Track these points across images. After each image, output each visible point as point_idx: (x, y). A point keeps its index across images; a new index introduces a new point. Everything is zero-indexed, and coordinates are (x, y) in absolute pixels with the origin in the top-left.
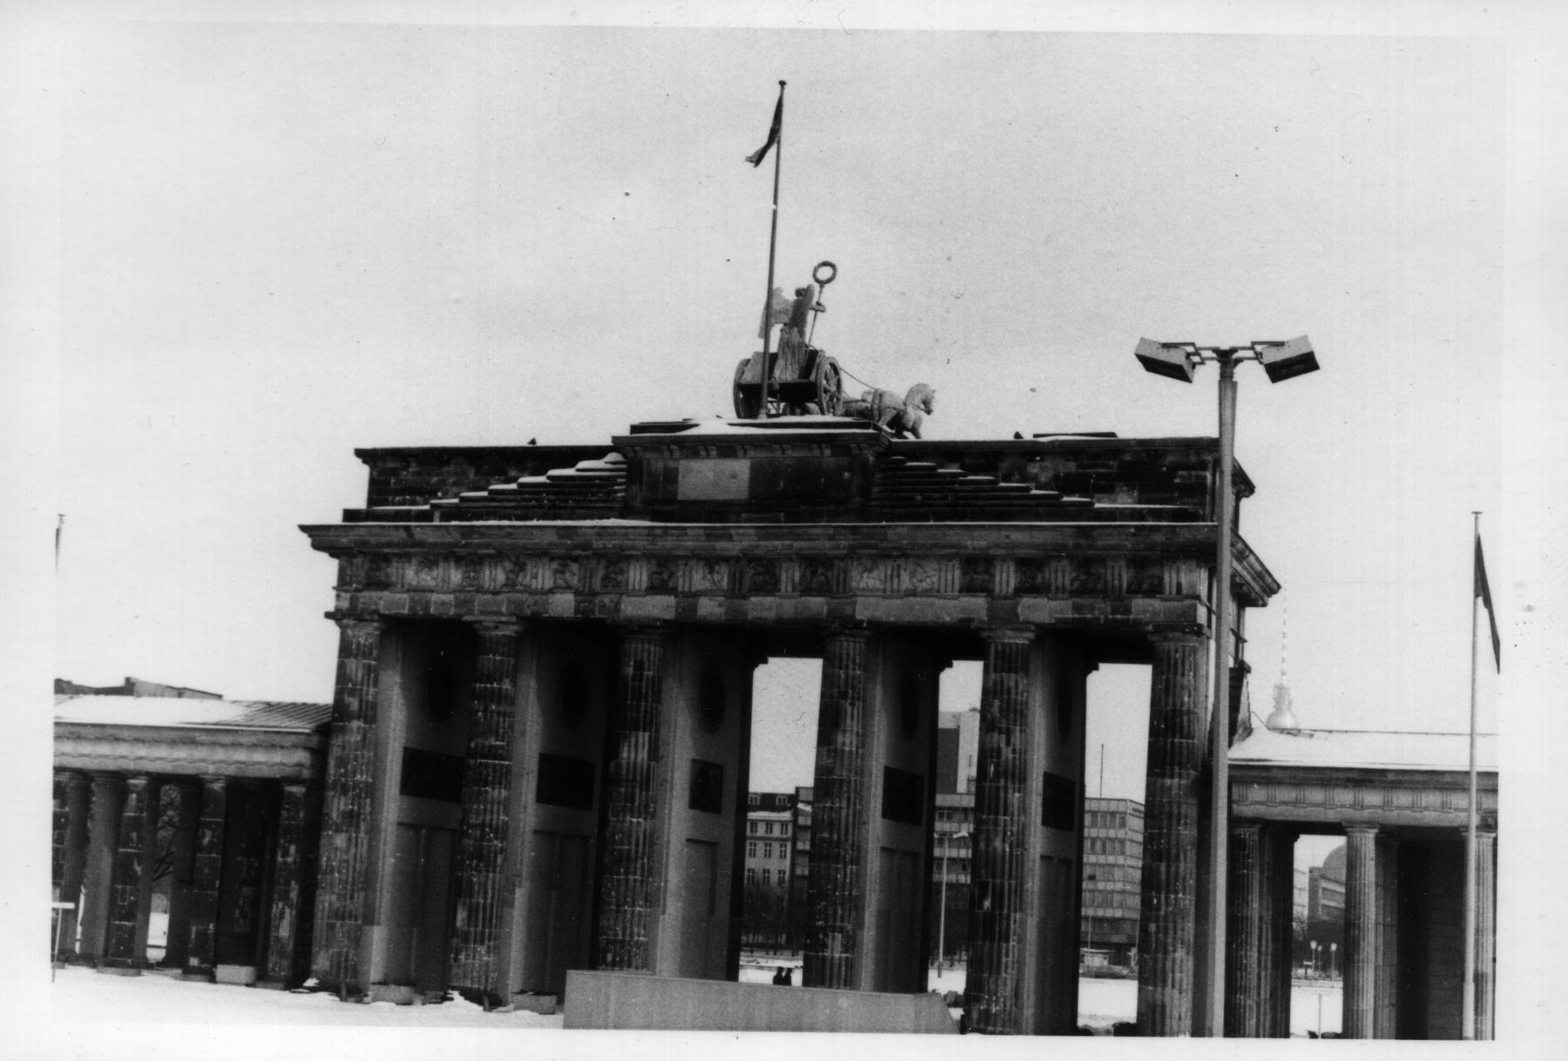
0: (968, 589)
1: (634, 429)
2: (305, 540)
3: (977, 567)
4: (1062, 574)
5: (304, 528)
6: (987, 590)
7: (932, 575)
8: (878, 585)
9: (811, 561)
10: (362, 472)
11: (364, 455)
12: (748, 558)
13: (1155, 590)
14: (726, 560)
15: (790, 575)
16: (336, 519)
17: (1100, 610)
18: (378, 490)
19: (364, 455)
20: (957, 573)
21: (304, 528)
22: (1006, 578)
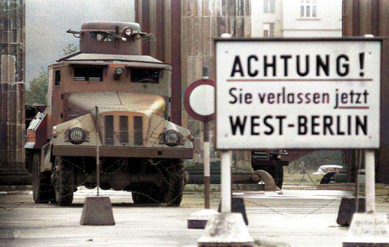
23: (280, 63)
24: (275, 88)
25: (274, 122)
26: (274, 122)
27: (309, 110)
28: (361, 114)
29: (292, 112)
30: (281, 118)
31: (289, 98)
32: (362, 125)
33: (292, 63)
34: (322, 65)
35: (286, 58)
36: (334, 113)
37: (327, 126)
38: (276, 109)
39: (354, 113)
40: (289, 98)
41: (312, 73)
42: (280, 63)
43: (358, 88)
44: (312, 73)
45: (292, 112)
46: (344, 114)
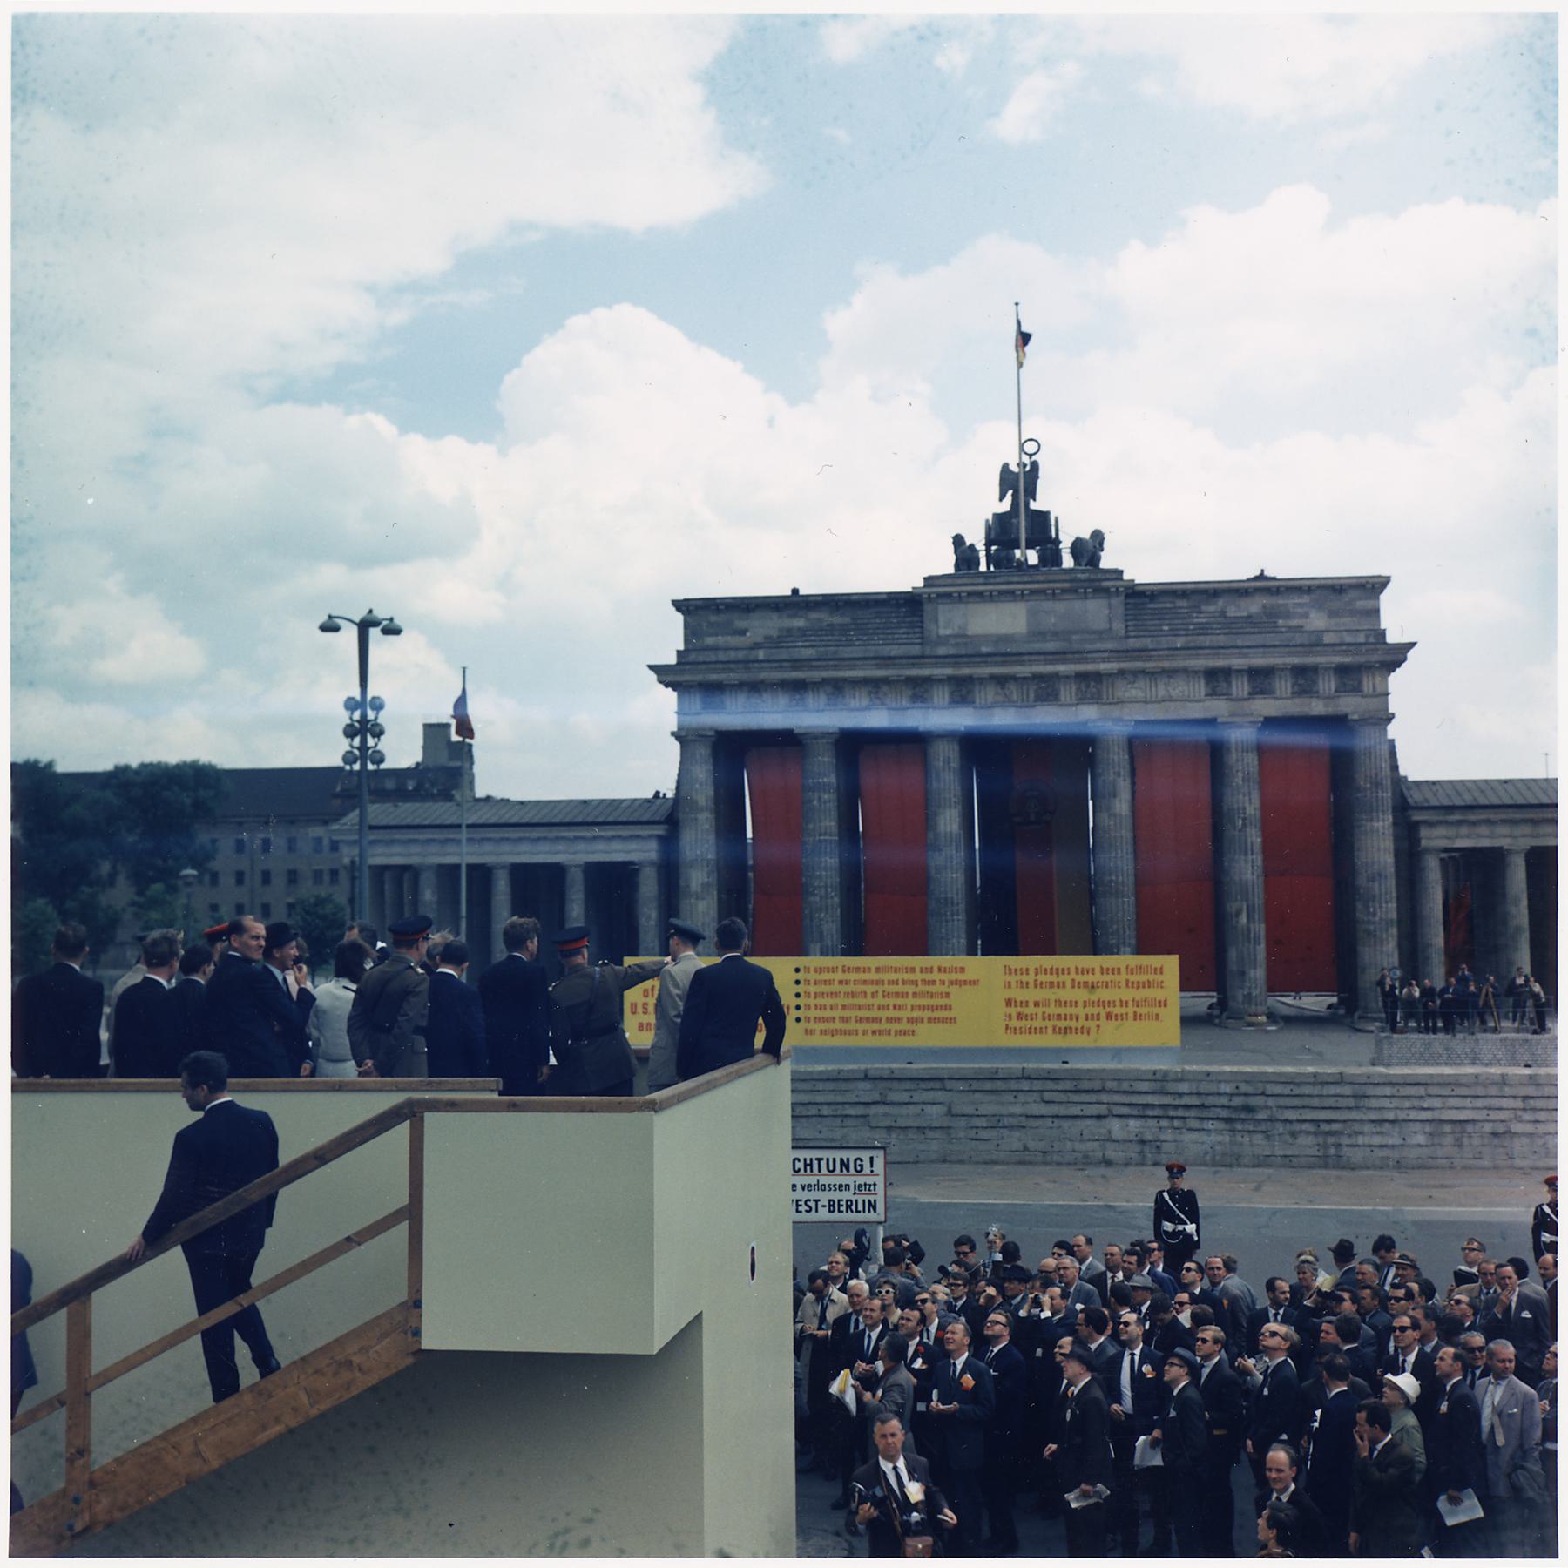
0: (1213, 694)
1: (929, 581)
2: (653, 676)
3: (1216, 679)
4: (1284, 685)
5: (651, 667)
6: (1228, 696)
7: (1180, 688)
8: (1141, 694)
9: (1082, 677)
10: (680, 617)
11: (679, 605)
12: (1038, 677)
13: (1357, 689)
14: (1013, 678)
15: (1067, 692)
16: (673, 660)
17: (1317, 708)
18: (690, 632)
19: (679, 605)
20: (1203, 682)
21: (651, 667)
22: (1241, 687)
23: (815, 1163)
24: (813, 1180)
25: (812, 1204)
26: (812, 1204)
27: (836, 1196)
28: (872, 1198)
29: (824, 1197)
30: (817, 1201)
31: (823, 1188)
32: (873, 1206)
33: (823, 1163)
34: (845, 1165)
35: (819, 1160)
36: (854, 1198)
37: (849, 1207)
38: (813, 1195)
39: (867, 1198)
40: (823, 1188)
41: (838, 1171)
42: (815, 1163)
43: (870, 1180)
44: (838, 1171)
45: (824, 1197)
46: (860, 1199)
